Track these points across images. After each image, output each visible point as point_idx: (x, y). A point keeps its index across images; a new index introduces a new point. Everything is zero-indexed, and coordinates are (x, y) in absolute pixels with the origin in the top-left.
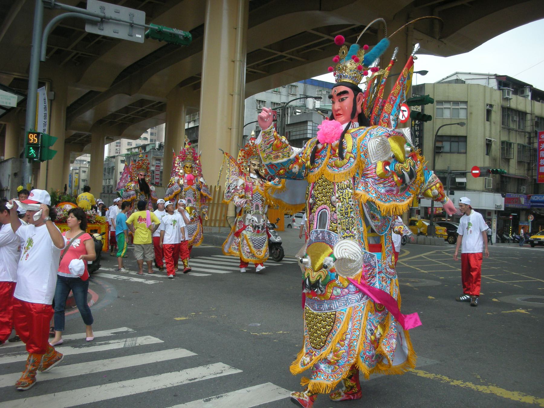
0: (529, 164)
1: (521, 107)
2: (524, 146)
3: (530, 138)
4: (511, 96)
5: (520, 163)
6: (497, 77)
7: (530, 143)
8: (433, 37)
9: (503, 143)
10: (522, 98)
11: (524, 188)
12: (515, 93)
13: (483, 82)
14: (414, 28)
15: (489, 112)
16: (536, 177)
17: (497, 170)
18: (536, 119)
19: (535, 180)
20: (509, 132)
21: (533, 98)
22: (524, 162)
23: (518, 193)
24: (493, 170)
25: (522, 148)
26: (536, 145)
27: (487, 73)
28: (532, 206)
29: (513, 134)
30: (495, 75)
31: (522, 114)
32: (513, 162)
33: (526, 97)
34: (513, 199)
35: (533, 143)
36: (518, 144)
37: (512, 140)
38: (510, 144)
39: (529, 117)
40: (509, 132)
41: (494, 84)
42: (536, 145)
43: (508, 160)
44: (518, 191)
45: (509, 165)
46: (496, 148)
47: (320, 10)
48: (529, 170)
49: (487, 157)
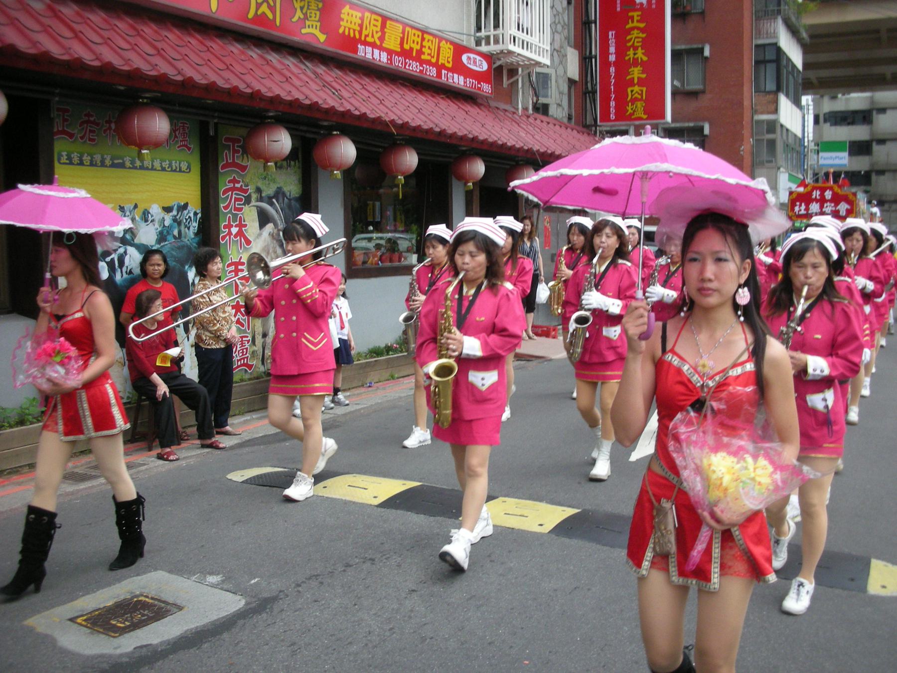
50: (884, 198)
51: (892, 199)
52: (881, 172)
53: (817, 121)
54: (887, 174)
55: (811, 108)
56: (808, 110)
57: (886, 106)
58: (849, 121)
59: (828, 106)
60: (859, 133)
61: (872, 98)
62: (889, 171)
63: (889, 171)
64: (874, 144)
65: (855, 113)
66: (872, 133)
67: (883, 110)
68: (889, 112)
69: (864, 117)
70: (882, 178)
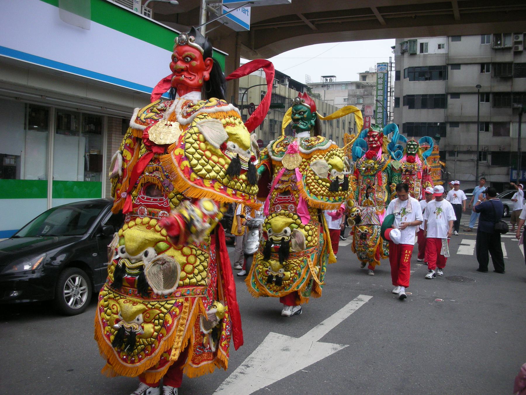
1: (282, 94)
4: (277, 85)
8: (251, 49)
9: (271, 121)
10: (283, 86)
12: (278, 83)
14: (242, 43)
20: (275, 113)
21: (290, 87)
29: (277, 113)
31: (284, 98)
33: (285, 85)
37: (276, 119)
38: (276, 121)
39: (287, 101)
40: (275, 113)
47: (177, 22)
49: (261, 131)
51: (465, 149)
52: (455, 124)
53: (398, 78)
54: (460, 126)
55: (393, 65)
57: (460, 62)
59: (408, 62)
60: (434, 87)
61: (447, 56)
62: (462, 123)
63: (462, 123)
64: (449, 97)
66: (447, 87)
67: (457, 66)
68: (462, 67)
69: (439, 72)
70: (455, 128)
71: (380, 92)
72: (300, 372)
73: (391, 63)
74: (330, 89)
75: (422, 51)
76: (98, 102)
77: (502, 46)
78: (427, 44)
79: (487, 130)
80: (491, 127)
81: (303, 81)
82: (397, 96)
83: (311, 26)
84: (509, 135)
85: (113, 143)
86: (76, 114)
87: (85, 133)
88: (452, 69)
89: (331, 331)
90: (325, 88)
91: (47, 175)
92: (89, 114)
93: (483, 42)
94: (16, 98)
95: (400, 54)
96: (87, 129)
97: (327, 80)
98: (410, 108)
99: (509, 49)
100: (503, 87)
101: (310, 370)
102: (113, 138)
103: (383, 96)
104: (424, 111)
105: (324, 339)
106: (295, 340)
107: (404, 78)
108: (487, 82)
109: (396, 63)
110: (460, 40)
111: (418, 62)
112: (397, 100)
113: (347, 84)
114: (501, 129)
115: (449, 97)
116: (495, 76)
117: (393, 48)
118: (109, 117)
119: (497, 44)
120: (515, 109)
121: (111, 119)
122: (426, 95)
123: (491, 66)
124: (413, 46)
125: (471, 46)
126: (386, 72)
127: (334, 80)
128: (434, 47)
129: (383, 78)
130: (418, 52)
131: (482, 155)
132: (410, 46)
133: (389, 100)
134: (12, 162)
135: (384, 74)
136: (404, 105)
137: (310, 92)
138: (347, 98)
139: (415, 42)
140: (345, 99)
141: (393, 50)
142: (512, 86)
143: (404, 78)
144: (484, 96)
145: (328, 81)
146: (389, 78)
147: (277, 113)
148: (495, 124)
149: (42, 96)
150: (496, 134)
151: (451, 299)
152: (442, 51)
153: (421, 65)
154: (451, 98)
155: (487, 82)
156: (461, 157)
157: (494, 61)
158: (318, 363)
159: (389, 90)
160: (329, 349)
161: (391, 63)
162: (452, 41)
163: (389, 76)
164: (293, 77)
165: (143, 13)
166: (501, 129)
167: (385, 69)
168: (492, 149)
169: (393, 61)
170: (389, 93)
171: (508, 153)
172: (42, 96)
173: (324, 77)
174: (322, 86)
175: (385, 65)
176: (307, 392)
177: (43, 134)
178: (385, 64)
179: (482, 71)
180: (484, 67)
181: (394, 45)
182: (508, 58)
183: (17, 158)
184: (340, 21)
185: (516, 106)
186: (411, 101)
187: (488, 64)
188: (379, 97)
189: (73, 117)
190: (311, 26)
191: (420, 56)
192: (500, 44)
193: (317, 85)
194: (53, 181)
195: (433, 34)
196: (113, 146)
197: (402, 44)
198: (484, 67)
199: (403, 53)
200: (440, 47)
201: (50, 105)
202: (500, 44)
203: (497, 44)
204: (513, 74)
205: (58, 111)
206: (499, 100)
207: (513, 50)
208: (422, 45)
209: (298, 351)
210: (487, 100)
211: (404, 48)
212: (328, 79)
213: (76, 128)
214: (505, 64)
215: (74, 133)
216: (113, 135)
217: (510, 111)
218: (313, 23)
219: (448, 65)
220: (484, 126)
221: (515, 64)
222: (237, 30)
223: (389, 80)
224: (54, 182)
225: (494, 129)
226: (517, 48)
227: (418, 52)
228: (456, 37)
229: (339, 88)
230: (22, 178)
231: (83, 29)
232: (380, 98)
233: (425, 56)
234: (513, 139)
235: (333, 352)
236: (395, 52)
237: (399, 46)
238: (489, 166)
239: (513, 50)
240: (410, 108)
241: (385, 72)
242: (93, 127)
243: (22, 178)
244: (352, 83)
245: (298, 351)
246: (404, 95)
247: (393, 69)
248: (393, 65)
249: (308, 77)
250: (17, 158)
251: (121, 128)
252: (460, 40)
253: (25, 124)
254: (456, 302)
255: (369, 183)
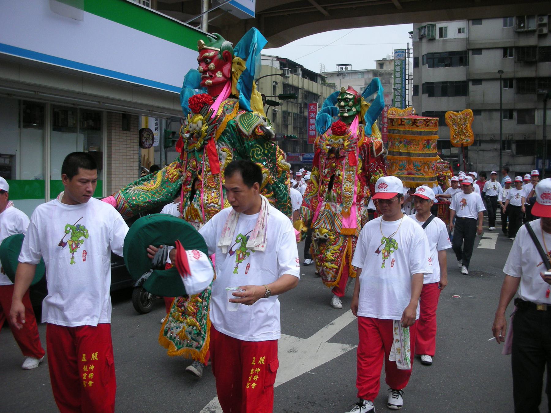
0: (300, 129)
1: (295, 84)
2: (298, 115)
3: (301, 108)
4: (290, 75)
5: (294, 128)
6: (279, 59)
7: (301, 112)
9: (284, 112)
11: (298, 149)
12: (291, 72)
13: (268, 63)
15: (274, 88)
16: (306, 140)
17: (291, 136)
18: (305, 93)
19: (305, 142)
20: (287, 104)
21: (303, 76)
22: (297, 127)
23: (293, 152)
24: (287, 136)
25: (296, 117)
26: (306, 114)
27: (272, 55)
28: (304, 162)
29: (290, 104)
30: (277, 57)
31: (296, 89)
32: (290, 128)
33: (298, 75)
34: (294, 157)
35: (304, 112)
36: (294, 113)
37: (290, 110)
38: (289, 113)
39: (300, 91)
40: (287, 104)
41: (277, 64)
42: (306, 114)
43: (286, 126)
44: (294, 151)
45: (287, 130)
46: (279, 116)
47: (183, 12)
48: (300, 134)
50: (481, 138)
51: (488, 138)
53: (416, 64)
54: (483, 113)
55: (411, 51)
56: (409, 53)
58: (446, 63)
59: (426, 48)
60: (455, 74)
61: (468, 40)
62: (485, 110)
63: (485, 110)
64: (470, 83)
65: (452, 54)
66: (468, 74)
67: (478, 51)
68: (484, 52)
69: (460, 58)
71: (398, 80)
72: (307, 374)
73: (409, 49)
74: (345, 78)
75: (441, 36)
76: (95, 96)
77: (526, 29)
78: (446, 28)
79: (511, 117)
80: (515, 114)
81: (317, 71)
82: (416, 84)
83: (323, 11)
84: (534, 123)
85: (113, 139)
86: (74, 110)
87: (83, 130)
88: (473, 54)
89: (341, 331)
90: (341, 77)
91: (44, 174)
92: (88, 110)
93: (505, 25)
94: (9, 94)
95: (418, 40)
96: (86, 126)
97: (342, 68)
98: (429, 96)
99: (533, 32)
100: (527, 73)
101: (317, 372)
102: (113, 134)
103: (401, 84)
104: (444, 99)
105: (334, 340)
106: (303, 341)
107: (423, 64)
108: (510, 68)
109: (414, 49)
110: (481, 24)
111: (437, 48)
112: (416, 89)
113: (363, 72)
114: (525, 116)
115: (470, 83)
116: (518, 60)
117: (411, 33)
118: (108, 112)
119: (520, 27)
120: (540, 96)
121: (110, 114)
122: (446, 83)
123: (514, 51)
124: (432, 31)
125: (493, 30)
126: (403, 59)
127: (350, 68)
128: (453, 32)
129: (401, 65)
130: (437, 37)
131: (505, 144)
132: (429, 31)
133: (407, 88)
134: (7, 161)
135: (402, 61)
136: (423, 93)
137: (325, 81)
138: (363, 86)
139: (434, 26)
140: (361, 88)
141: (410, 36)
142: (536, 70)
143: (423, 64)
144: (507, 82)
145: (344, 69)
146: (407, 65)
147: (290, 104)
148: (520, 111)
149: (35, 92)
150: (521, 121)
151: (470, 295)
152: (463, 36)
153: (440, 51)
154: (473, 85)
155: (510, 68)
156: (484, 146)
157: (517, 45)
158: (325, 364)
159: (407, 78)
160: (338, 350)
161: (409, 49)
162: (473, 24)
163: (407, 63)
164: (306, 67)
165: (142, 2)
166: (525, 116)
167: (403, 55)
168: (517, 138)
169: (411, 47)
170: (407, 81)
171: (534, 141)
172: (35, 92)
173: (339, 65)
174: (338, 75)
175: (403, 52)
176: (312, 396)
177: (39, 132)
178: (402, 51)
179: (505, 55)
180: (506, 51)
181: (411, 29)
182: (532, 41)
183: (12, 157)
184: (354, 7)
185: (541, 91)
186: (430, 89)
187: (511, 48)
188: (396, 85)
189: (70, 113)
190: (323, 11)
191: (439, 41)
192: (524, 27)
193: (332, 74)
194: (51, 180)
195: (452, 18)
196: (113, 142)
197: (420, 29)
198: (506, 51)
199: (421, 38)
200: (460, 31)
201: (45, 101)
202: (524, 27)
203: (520, 27)
204: (537, 57)
205: (54, 107)
206: (523, 85)
207: (537, 33)
208: (441, 29)
209: (305, 352)
210: (511, 87)
211: (422, 33)
212: (344, 67)
213: (74, 124)
214: (529, 48)
215: (72, 130)
216: (113, 131)
217: (534, 97)
218: (325, 8)
219: (469, 50)
220: (508, 113)
221: (540, 47)
222: (242, 18)
223: (407, 68)
224: (52, 181)
225: (518, 116)
226: (541, 31)
227: (437, 37)
228: (477, 20)
229: (355, 77)
230: (18, 178)
231: (76, 20)
232: (398, 86)
233: (443, 40)
234: (538, 126)
235: (342, 353)
236: (412, 37)
237: (417, 31)
238: (513, 156)
239: (537, 33)
240: (429, 96)
241: (403, 59)
242: (91, 123)
243: (18, 178)
244: (368, 71)
245: (305, 352)
246: (424, 82)
247: (411, 55)
248: (411, 51)
249: (322, 66)
250: (12, 157)
251: (121, 123)
252: (481, 24)
253: (19, 121)
254: (474, 298)
255: (195, 168)
